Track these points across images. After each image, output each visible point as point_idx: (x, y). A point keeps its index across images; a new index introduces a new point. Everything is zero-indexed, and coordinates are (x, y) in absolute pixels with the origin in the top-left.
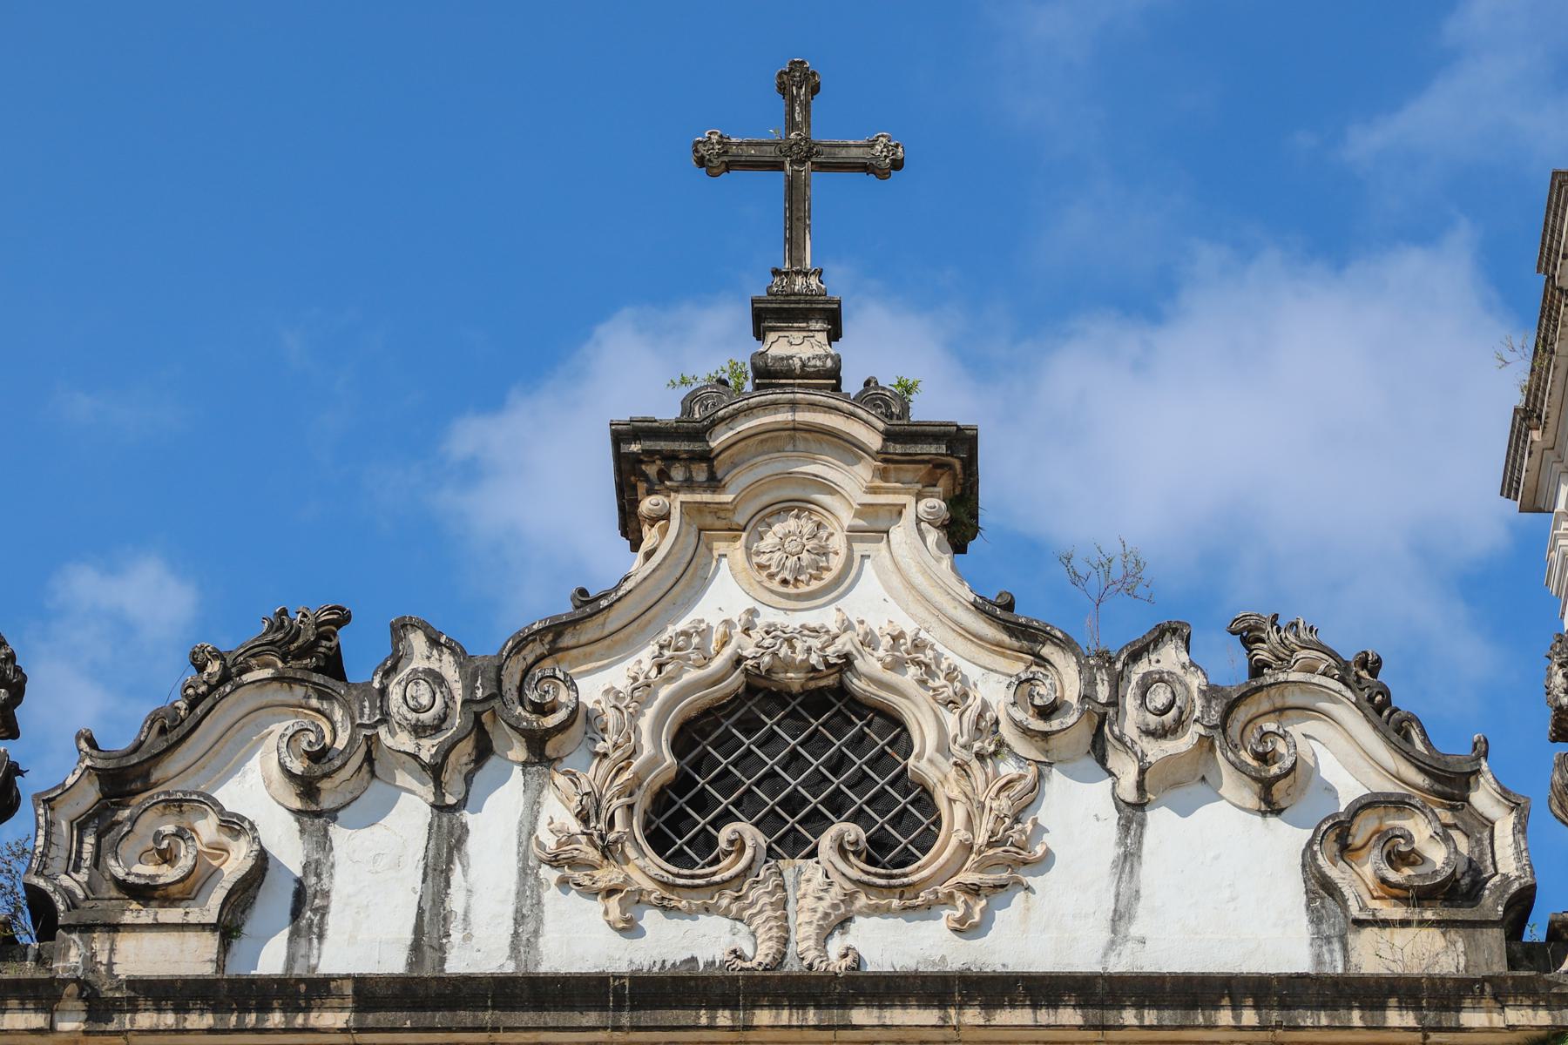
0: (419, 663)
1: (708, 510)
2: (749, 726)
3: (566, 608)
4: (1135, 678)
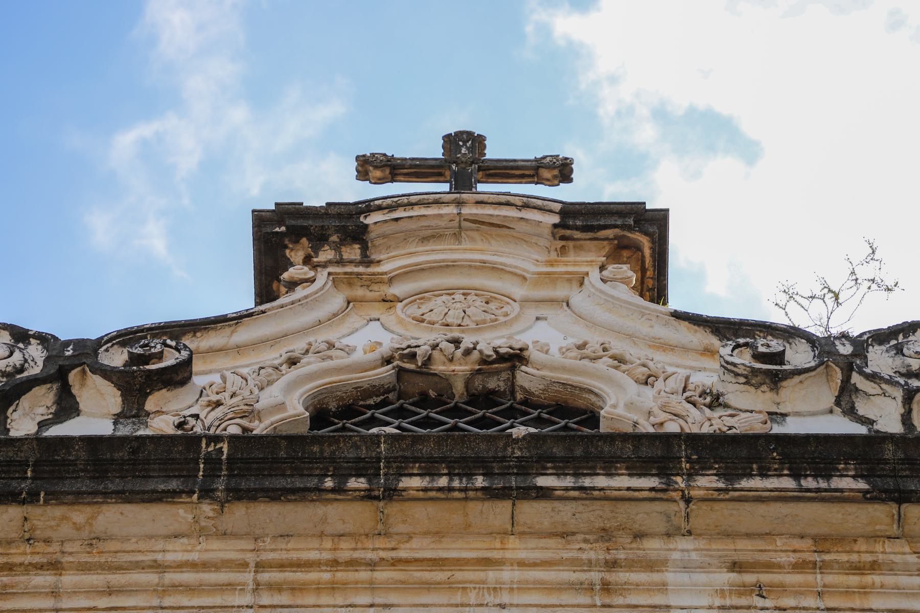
1: (359, 284)
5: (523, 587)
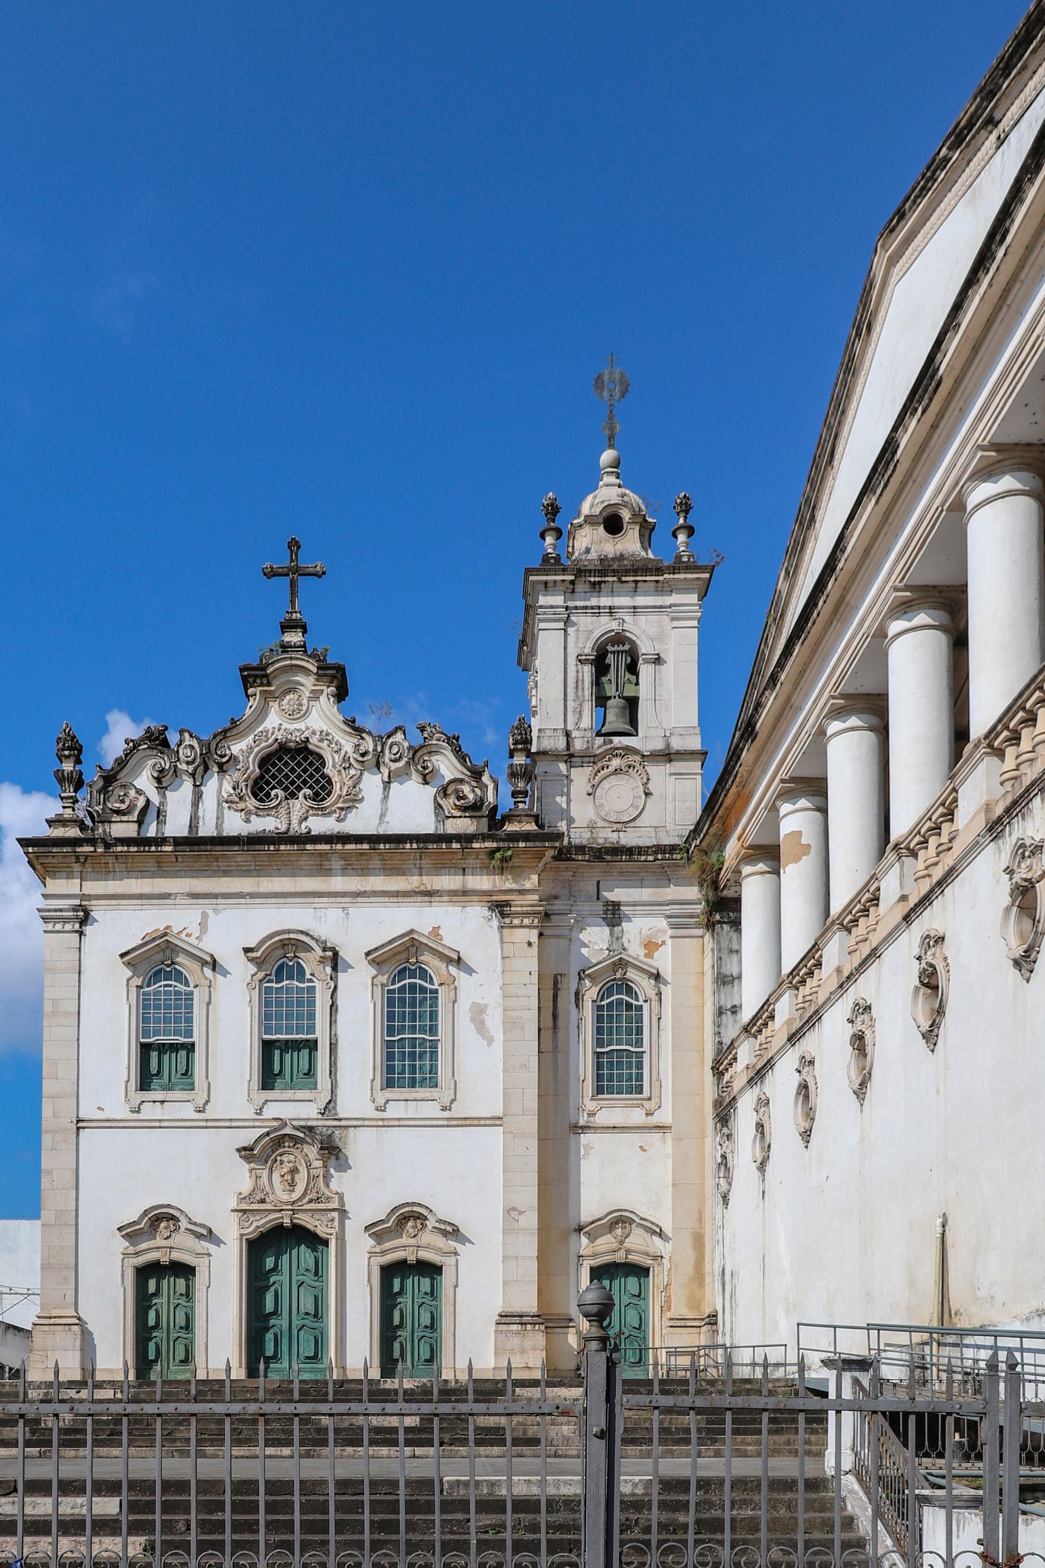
0: (187, 743)
2: (280, 759)
3: (228, 725)
4: (389, 744)
5: (305, 865)
